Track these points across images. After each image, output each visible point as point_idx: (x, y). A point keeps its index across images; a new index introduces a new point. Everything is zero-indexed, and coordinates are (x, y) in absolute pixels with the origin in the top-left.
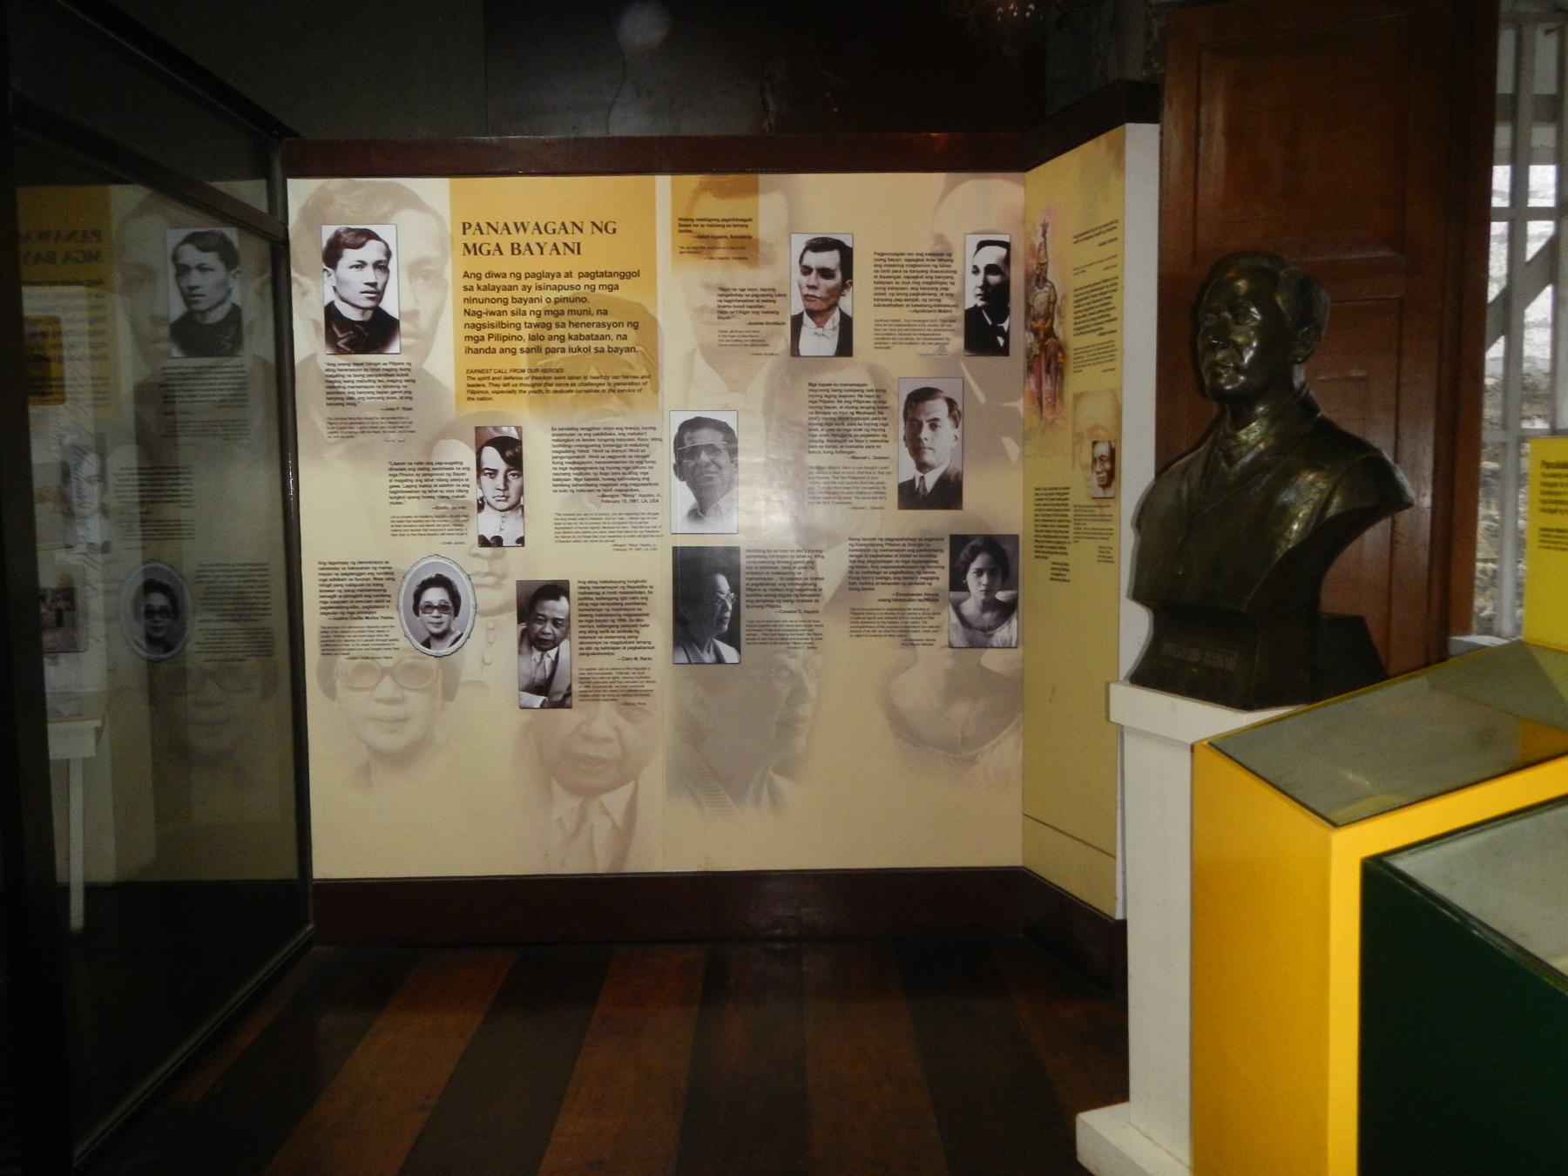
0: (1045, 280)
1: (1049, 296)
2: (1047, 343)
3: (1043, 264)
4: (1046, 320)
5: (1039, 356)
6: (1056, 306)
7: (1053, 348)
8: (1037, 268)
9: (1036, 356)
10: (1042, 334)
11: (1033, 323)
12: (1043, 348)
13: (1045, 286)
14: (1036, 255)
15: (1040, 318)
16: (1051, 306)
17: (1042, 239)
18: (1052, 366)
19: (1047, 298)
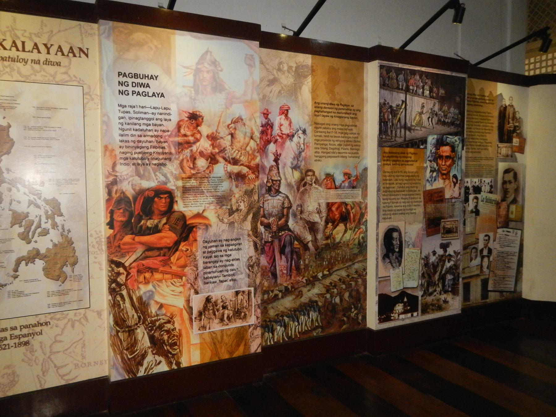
0: (278, 192)
1: (283, 203)
2: (280, 234)
3: (276, 181)
4: (280, 219)
5: (272, 242)
6: (291, 210)
7: (288, 238)
8: (267, 182)
9: (266, 242)
10: (274, 228)
11: (263, 219)
12: (275, 236)
13: (278, 195)
14: (267, 173)
15: (273, 216)
16: (285, 210)
17: (274, 164)
18: (288, 250)
19: (280, 204)
